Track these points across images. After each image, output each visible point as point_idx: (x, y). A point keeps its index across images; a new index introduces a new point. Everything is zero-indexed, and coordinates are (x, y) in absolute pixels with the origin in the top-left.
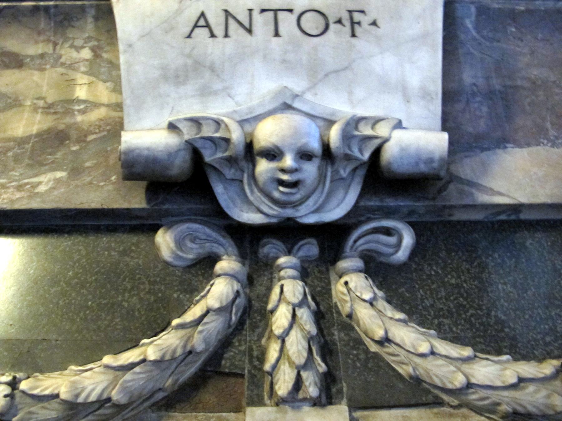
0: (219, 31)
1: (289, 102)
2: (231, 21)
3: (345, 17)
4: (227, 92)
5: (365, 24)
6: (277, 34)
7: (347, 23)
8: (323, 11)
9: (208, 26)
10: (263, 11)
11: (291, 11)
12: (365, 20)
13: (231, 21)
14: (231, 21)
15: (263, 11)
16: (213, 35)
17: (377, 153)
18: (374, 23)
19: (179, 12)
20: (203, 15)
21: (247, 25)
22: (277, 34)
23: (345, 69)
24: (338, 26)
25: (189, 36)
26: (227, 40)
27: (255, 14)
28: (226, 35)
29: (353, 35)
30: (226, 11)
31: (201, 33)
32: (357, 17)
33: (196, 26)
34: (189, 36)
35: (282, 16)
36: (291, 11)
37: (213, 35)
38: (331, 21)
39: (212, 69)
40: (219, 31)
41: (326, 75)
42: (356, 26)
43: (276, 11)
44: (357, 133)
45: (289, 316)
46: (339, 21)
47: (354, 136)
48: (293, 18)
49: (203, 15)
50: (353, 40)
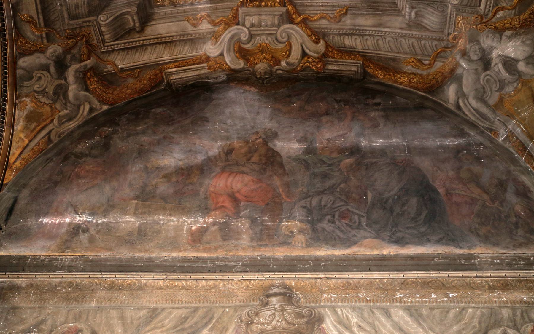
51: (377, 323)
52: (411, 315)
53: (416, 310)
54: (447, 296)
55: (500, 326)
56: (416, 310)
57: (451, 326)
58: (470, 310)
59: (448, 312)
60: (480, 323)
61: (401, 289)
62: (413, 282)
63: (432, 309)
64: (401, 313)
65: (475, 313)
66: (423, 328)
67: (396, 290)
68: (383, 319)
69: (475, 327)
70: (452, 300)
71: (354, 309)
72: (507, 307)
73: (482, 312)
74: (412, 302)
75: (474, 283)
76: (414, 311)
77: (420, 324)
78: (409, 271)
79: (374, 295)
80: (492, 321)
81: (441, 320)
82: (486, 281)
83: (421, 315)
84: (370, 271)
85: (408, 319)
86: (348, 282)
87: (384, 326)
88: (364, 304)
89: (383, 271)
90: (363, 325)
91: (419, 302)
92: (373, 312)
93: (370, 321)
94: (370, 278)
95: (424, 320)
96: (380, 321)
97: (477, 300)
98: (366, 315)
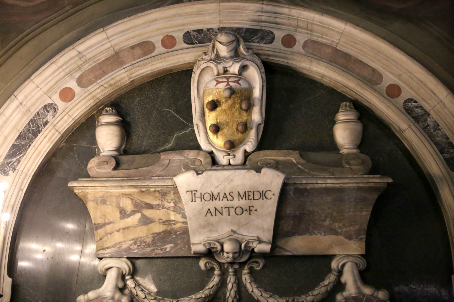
0: (214, 214)
1: (232, 235)
2: (217, 211)
3: (248, 208)
4: (216, 231)
5: (253, 211)
6: (229, 215)
7: (248, 210)
8: (242, 207)
9: (211, 213)
10: (225, 208)
11: (233, 207)
12: (253, 209)
13: (217, 211)
14: (217, 210)
15: (225, 208)
16: (212, 215)
17: (253, 249)
18: (256, 210)
19: (203, 208)
20: (209, 209)
21: (221, 212)
22: (229, 215)
23: (247, 224)
24: (246, 211)
25: (206, 216)
26: (216, 217)
27: (223, 209)
28: (216, 215)
29: (250, 214)
30: (215, 208)
31: (209, 215)
32: (251, 208)
33: (207, 213)
34: (206, 216)
35: (230, 209)
36: (233, 207)
37: (212, 215)
38: (244, 210)
39: (212, 225)
40: (214, 214)
41: (242, 226)
42: (251, 212)
43: (229, 208)
44: (249, 245)
45: (232, 286)
46: (246, 210)
47: (248, 246)
48: (233, 210)
49: (209, 209)
50: (250, 216)
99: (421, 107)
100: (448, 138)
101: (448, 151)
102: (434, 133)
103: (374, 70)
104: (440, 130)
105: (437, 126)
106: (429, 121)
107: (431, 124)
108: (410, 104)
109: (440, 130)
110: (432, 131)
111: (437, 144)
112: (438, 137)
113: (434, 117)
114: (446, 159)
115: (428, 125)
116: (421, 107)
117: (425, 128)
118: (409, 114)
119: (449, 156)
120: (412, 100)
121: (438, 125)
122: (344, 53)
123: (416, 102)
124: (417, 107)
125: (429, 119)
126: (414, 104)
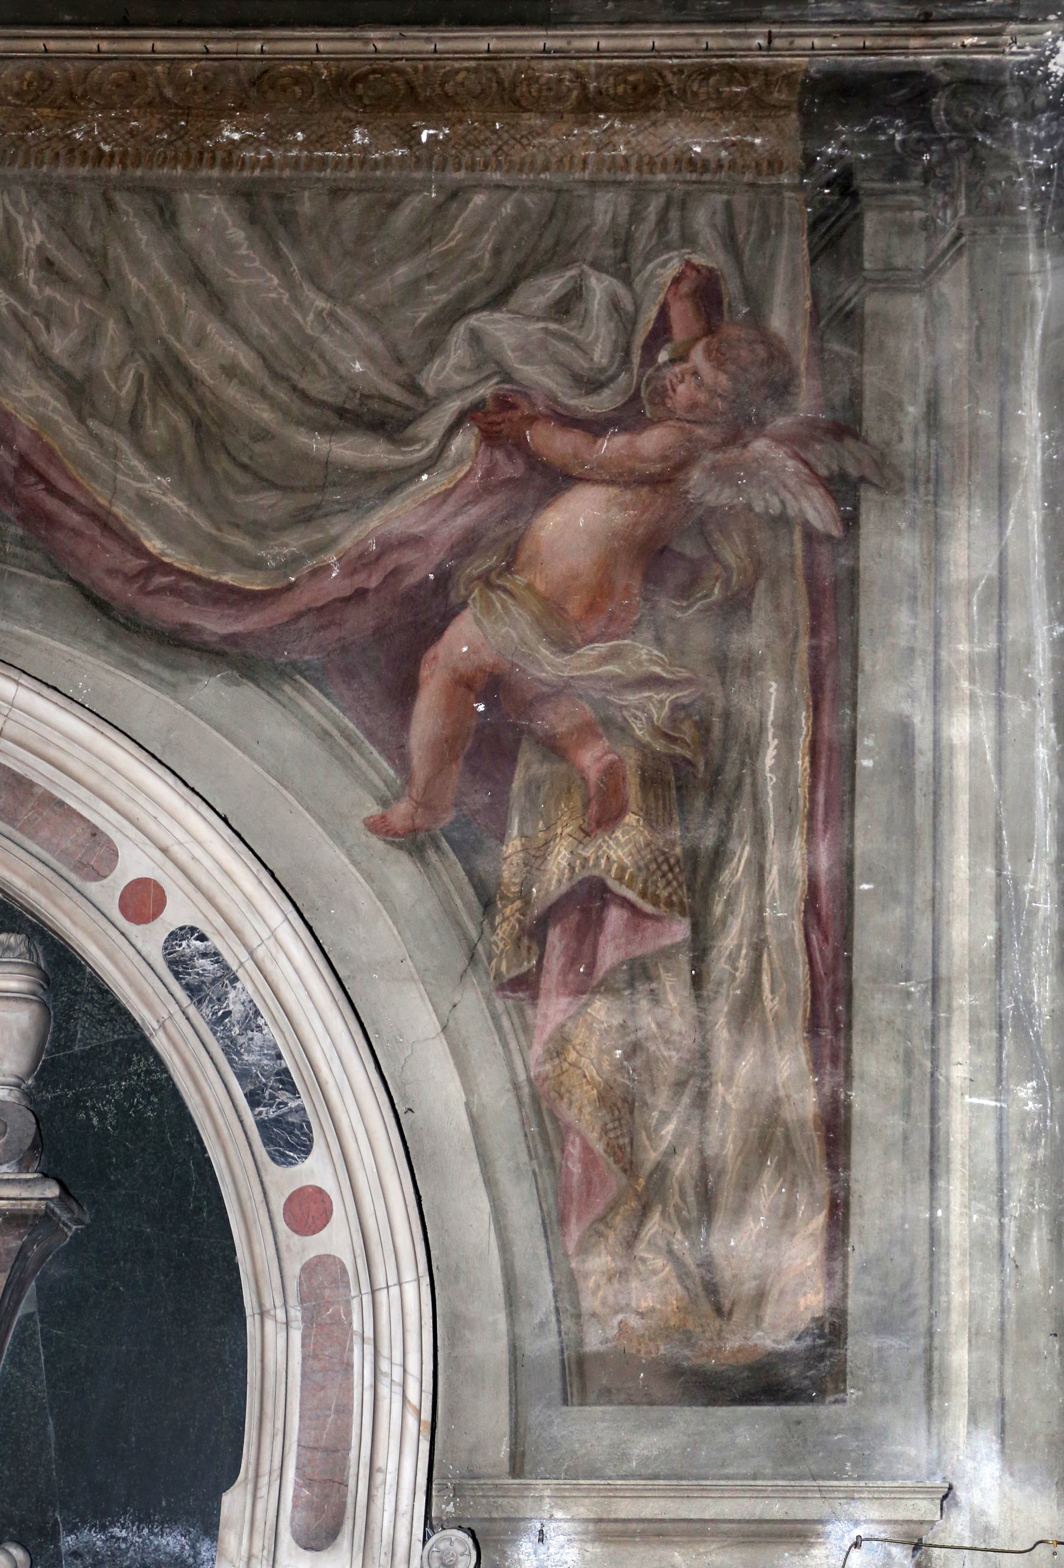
51: (116, 250)
52: (253, 219)
53: (278, 198)
54: (410, 139)
55: (566, 265)
56: (278, 198)
57: (392, 262)
58: (479, 199)
59: (393, 206)
60: (497, 252)
61: (242, 107)
62: (298, 78)
63: (337, 193)
64: (218, 208)
65: (492, 209)
66: (285, 274)
67: (223, 113)
68: (143, 235)
69: (475, 266)
70: (423, 158)
71: (42, 189)
72: (621, 184)
73: (520, 205)
74: (270, 163)
75: (531, 80)
76: (267, 203)
77: (276, 255)
78: (284, 24)
79: (132, 133)
80: (548, 241)
81: (361, 240)
82: (578, 75)
83: (288, 219)
84: (125, 24)
85: (238, 234)
86: (42, 76)
87: (140, 262)
88: (83, 171)
89: (180, 25)
90: (63, 259)
91: (296, 163)
92: (110, 205)
93: (94, 241)
94: (131, 57)
95: (296, 241)
96: (129, 244)
97: (517, 154)
98: (83, 217)
99: (215, 955)
100: (279, 1056)
101: (273, 1097)
102: (241, 1040)
103: (95, 832)
104: (259, 1028)
105: (252, 1019)
106: (234, 1002)
107: (237, 1010)
108: (184, 943)
109: (259, 1028)
110: (236, 1030)
111: (243, 1075)
112: (250, 1051)
113: (250, 988)
114: (262, 1125)
115: (228, 1014)
116: (216, 954)
117: (219, 1021)
118: (176, 975)
119: (272, 1113)
120: (193, 929)
121: (257, 1013)
122: (14, 774)
123: (202, 938)
124: (204, 955)
125: (232, 995)
126: (198, 943)
